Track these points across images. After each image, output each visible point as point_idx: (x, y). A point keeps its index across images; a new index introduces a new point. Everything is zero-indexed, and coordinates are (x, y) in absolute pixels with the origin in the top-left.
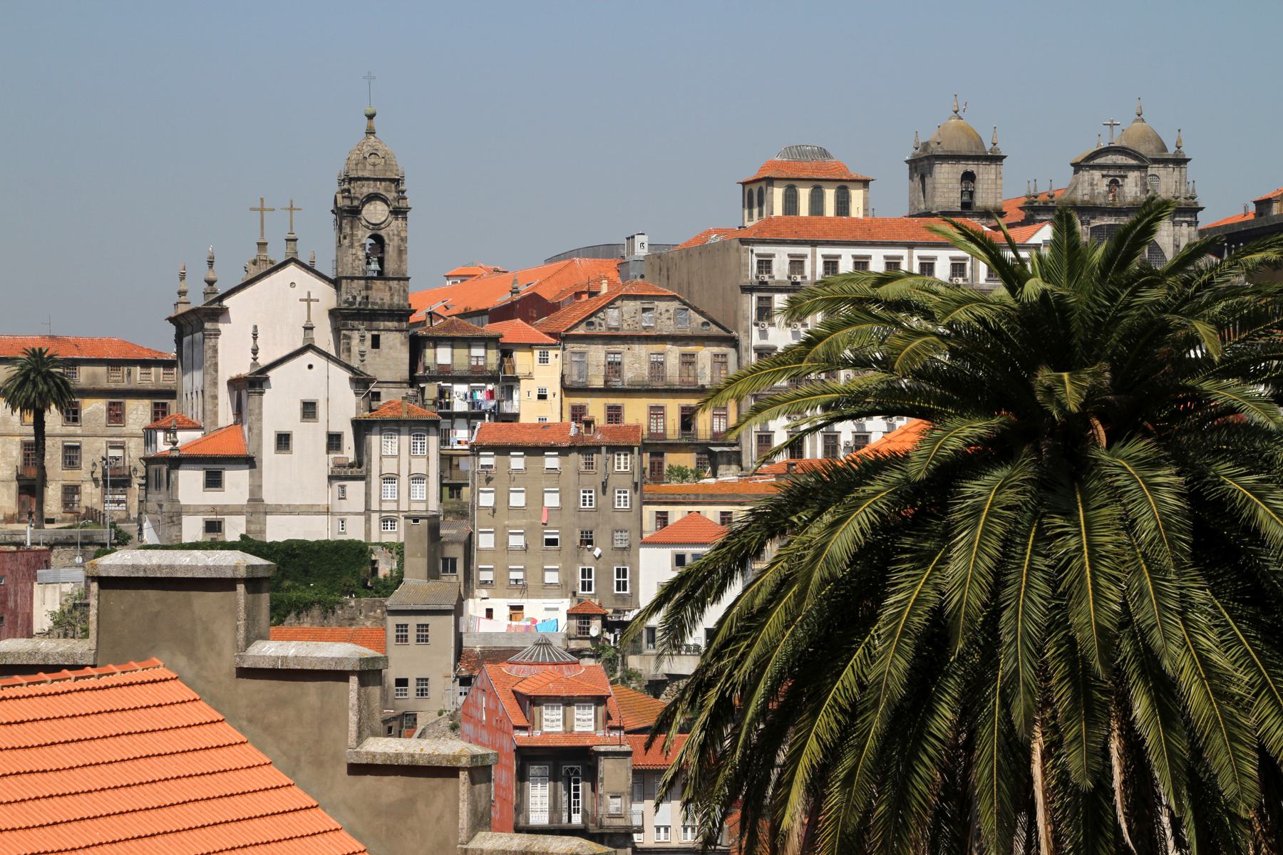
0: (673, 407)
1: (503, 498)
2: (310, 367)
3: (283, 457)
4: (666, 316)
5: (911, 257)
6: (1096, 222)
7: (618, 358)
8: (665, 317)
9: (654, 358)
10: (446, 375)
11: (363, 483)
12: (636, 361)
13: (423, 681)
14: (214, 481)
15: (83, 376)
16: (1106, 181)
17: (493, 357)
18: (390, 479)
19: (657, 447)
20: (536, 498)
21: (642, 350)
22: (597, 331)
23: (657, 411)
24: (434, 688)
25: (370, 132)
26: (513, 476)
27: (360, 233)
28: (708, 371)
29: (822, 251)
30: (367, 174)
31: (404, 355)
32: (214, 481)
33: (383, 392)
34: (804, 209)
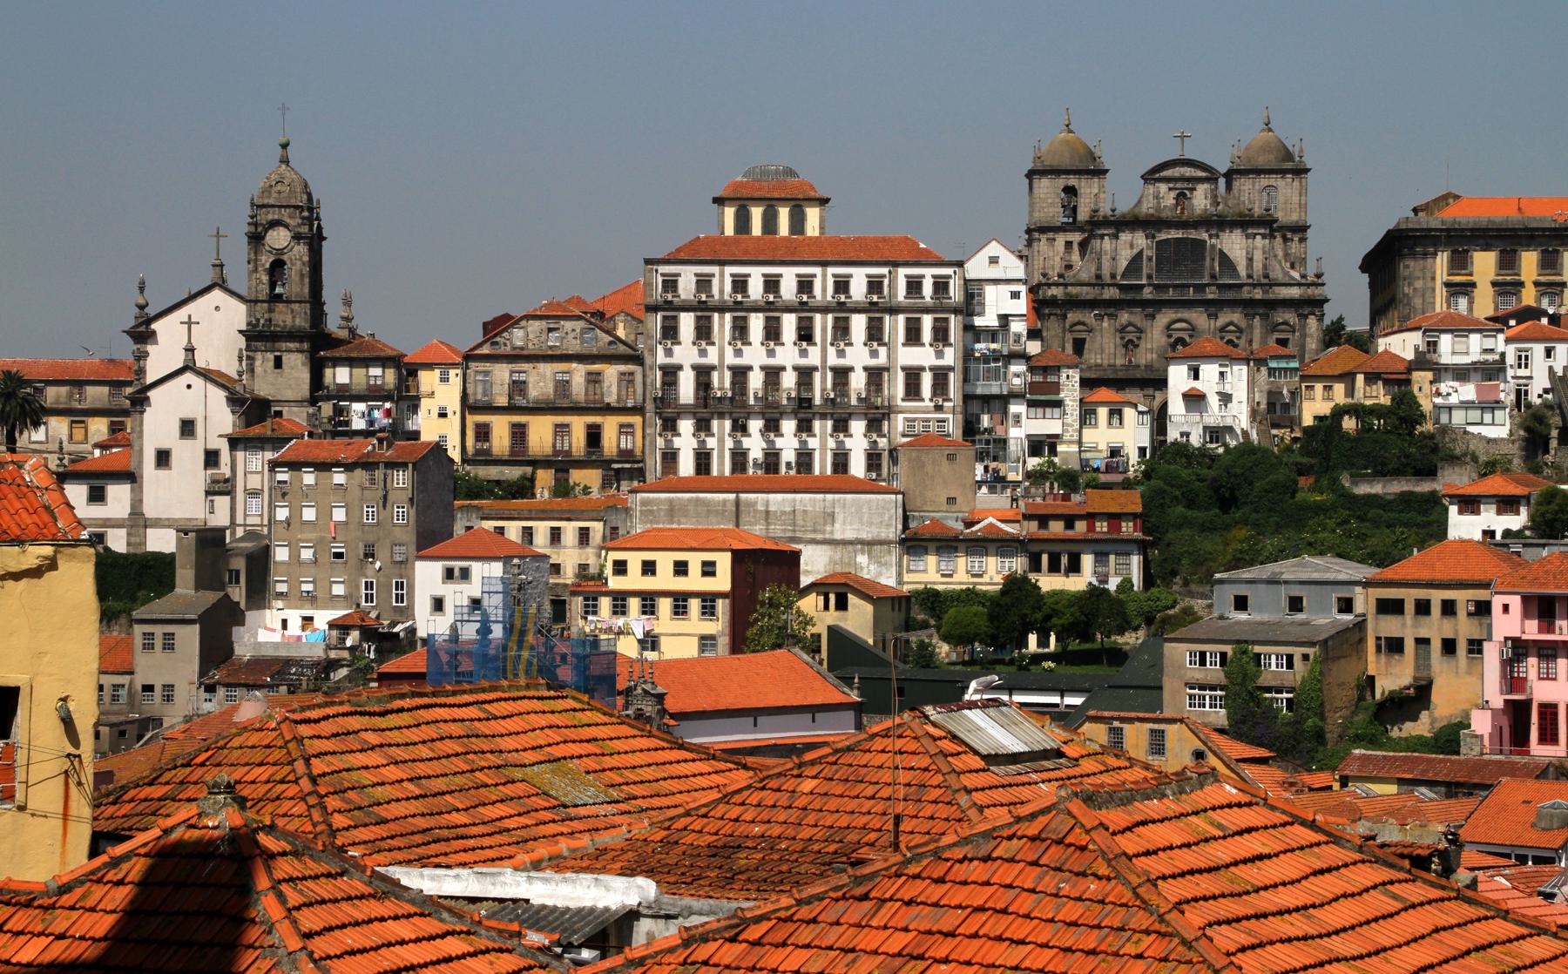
0: (578, 426)
1: (296, 512)
2: (189, 387)
3: (162, 473)
4: (572, 335)
5: (824, 276)
6: (1163, 236)
7: (523, 377)
8: (571, 335)
9: (559, 377)
10: (346, 394)
11: (228, 498)
12: (541, 380)
13: (169, 688)
14: (97, 496)
15: (53, 395)
16: (1173, 194)
17: (390, 377)
18: (254, 493)
19: (561, 464)
20: (325, 513)
21: (547, 369)
22: (502, 350)
23: (561, 430)
24: (180, 694)
25: (285, 161)
26: (307, 494)
27: (264, 258)
28: (614, 389)
29: (729, 270)
30: (272, 201)
31: (305, 375)
32: (97, 496)
33: (285, 410)
34: (757, 229)
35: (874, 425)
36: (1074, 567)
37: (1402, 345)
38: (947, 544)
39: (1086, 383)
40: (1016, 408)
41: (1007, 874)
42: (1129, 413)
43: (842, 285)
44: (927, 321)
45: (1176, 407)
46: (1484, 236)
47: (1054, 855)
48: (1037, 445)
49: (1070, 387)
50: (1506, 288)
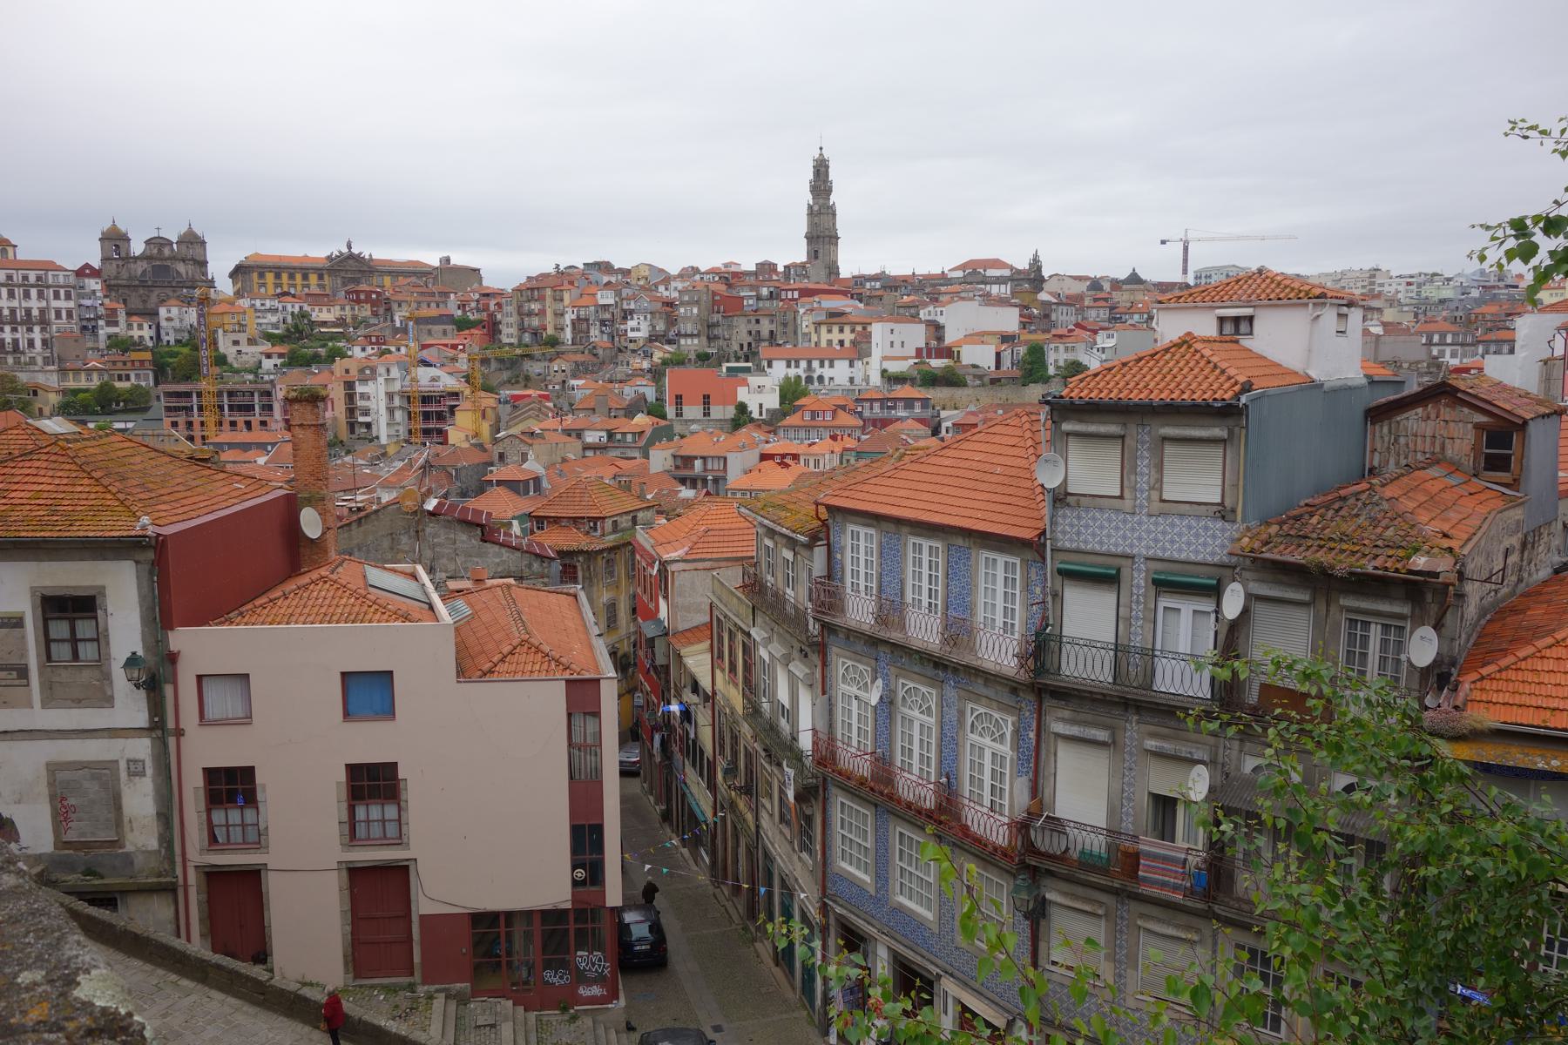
35: (43, 330)
36: (128, 378)
37: (244, 303)
38: (77, 371)
39: (129, 314)
40: (101, 323)
41: (37, 464)
42: (146, 326)
43: (25, 278)
44: (62, 292)
45: (163, 323)
46: (271, 268)
47: (53, 458)
48: (109, 337)
49: (122, 317)
50: (276, 286)
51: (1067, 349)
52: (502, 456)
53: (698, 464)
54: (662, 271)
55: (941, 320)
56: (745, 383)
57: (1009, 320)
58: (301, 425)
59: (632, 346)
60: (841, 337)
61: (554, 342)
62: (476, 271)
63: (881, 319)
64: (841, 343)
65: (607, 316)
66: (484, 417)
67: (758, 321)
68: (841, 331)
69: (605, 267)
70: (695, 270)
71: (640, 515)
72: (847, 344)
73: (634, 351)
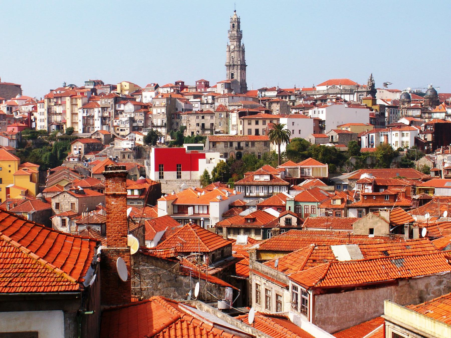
51: (403, 135)
52: (57, 205)
53: (190, 210)
54: (135, 86)
55: (322, 117)
56: (203, 156)
57: (363, 116)
58: (114, 196)
59: (122, 133)
60: (257, 127)
61: (71, 131)
62: (20, 86)
63: (283, 116)
64: (257, 131)
65: (106, 114)
66: (31, 180)
67: (203, 118)
68: (257, 123)
69: (97, 83)
70: (157, 87)
71: (225, 249)
72: (260, 132)
73: (123, 136)
